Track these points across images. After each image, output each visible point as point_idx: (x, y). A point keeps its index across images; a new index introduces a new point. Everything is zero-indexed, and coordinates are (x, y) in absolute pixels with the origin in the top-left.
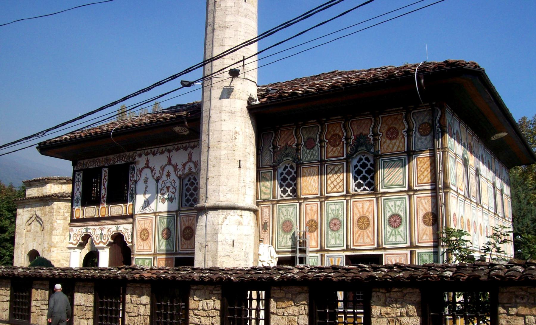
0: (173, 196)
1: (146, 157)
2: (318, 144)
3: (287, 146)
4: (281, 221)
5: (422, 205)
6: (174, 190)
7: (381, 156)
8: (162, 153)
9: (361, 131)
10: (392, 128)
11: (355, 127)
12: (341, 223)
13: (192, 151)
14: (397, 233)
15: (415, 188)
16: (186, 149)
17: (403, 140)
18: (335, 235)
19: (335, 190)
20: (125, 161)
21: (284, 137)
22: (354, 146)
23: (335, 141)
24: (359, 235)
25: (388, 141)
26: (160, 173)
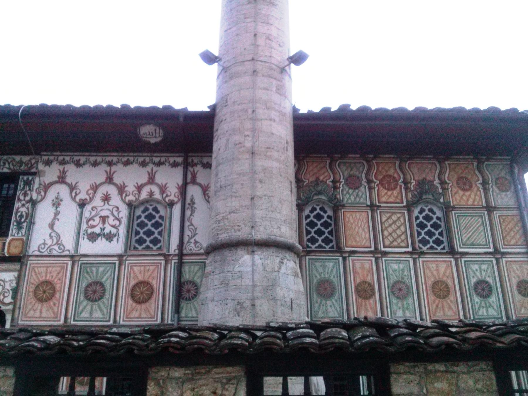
0: (114, 231)
1: (61, 168)
2: (366, 184)
3: (317, 182)
4: (315, 281)
5: (514, 271)
6: (117, 223)
7: (454, 208)
8: (95, 164)
9: (424, 176)
10: (462, 178)
11: (415, 170)
12: (409, 289)
13: (155, 169)
14: (488, 305)
15: (502, 250)
16: (144, 164)
17: (478, 193)
18: (403, 305)
19: (395, 243)
20: (9, 168)
21: (312, 170)
22: (416, 193)
23: (389, 183)
24: (437, 306)
25: (461, 192)
26: (87, 193)
